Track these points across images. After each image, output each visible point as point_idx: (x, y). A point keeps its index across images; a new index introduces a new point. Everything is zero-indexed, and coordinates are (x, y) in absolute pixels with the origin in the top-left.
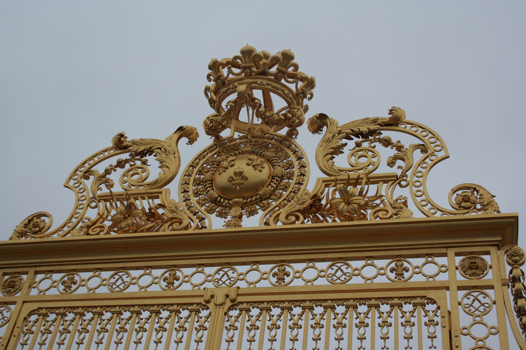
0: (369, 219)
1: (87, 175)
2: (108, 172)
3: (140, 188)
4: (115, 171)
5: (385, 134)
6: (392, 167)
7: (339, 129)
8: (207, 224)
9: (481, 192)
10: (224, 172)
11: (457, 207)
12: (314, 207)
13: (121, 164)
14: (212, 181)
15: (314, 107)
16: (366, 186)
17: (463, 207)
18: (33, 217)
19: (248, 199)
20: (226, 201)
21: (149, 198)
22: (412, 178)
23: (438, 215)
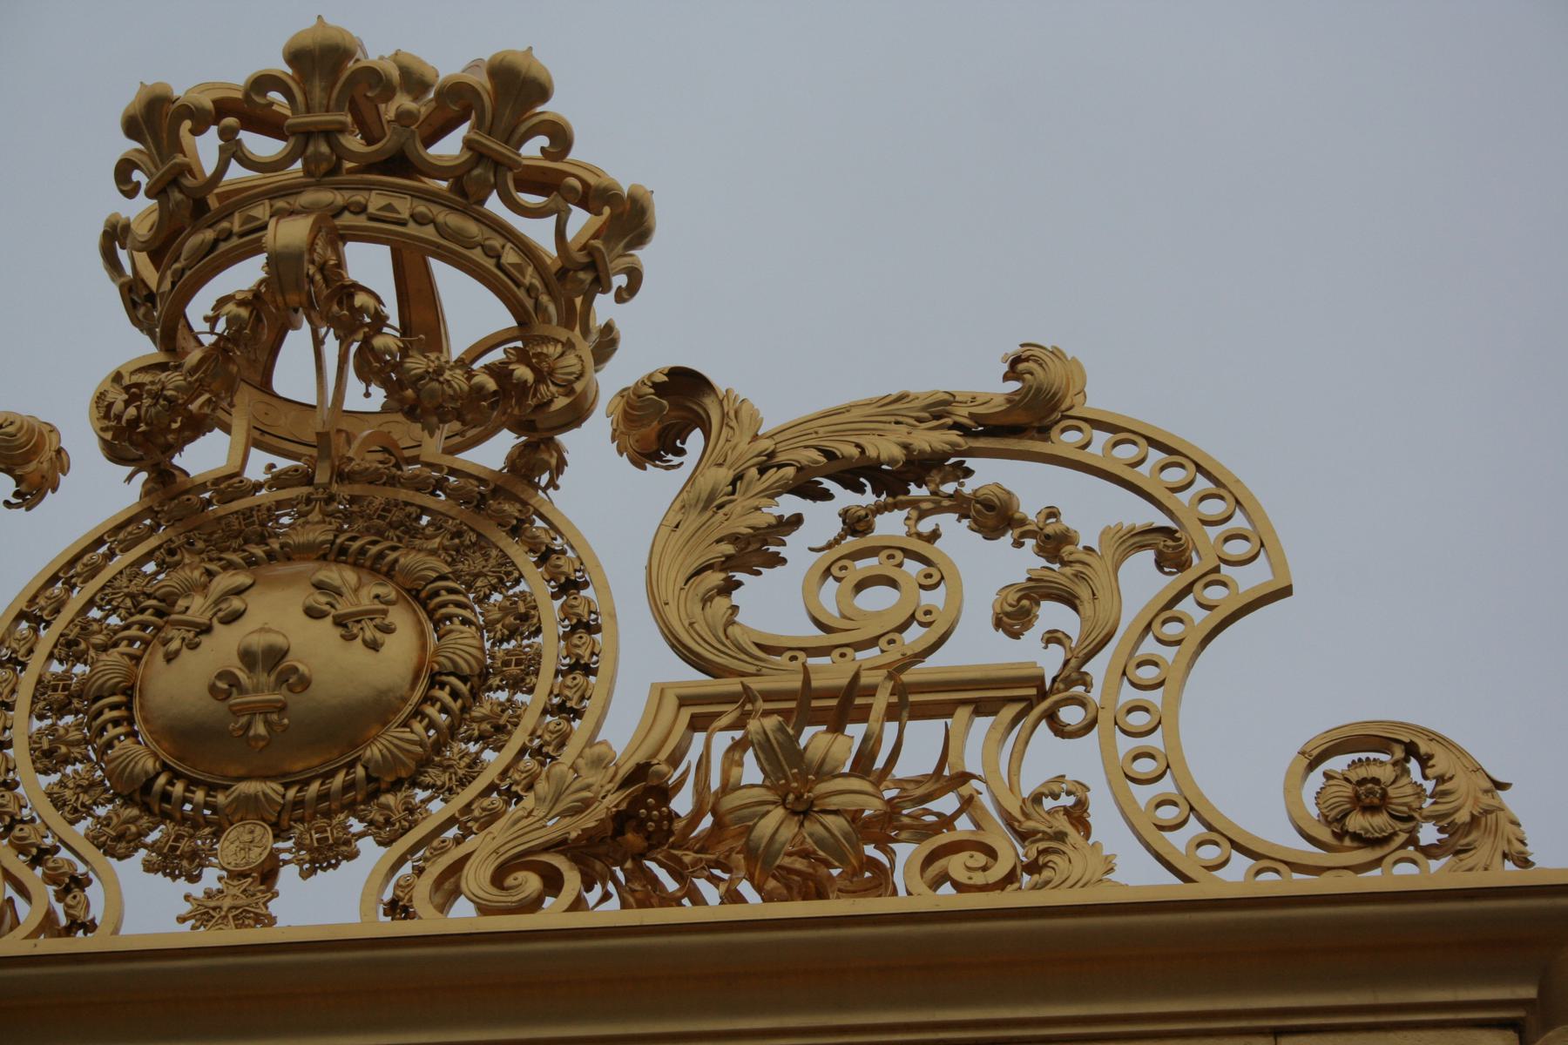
0: (902, 892)
5: (988, 473)
6: (1016, 635)
7: (767, 445)
8: (97, 912)
9: (1441, 764)
10: (194, 646)
11: (1325, 834)
12: (634, 825)
14: (129, 691)
15: (645, 335)
16: (891, 729)
17: (1356, 837)
19: (307, 783)
20: (200, 795)
22: (1111, 691)
23: (1236, 875)
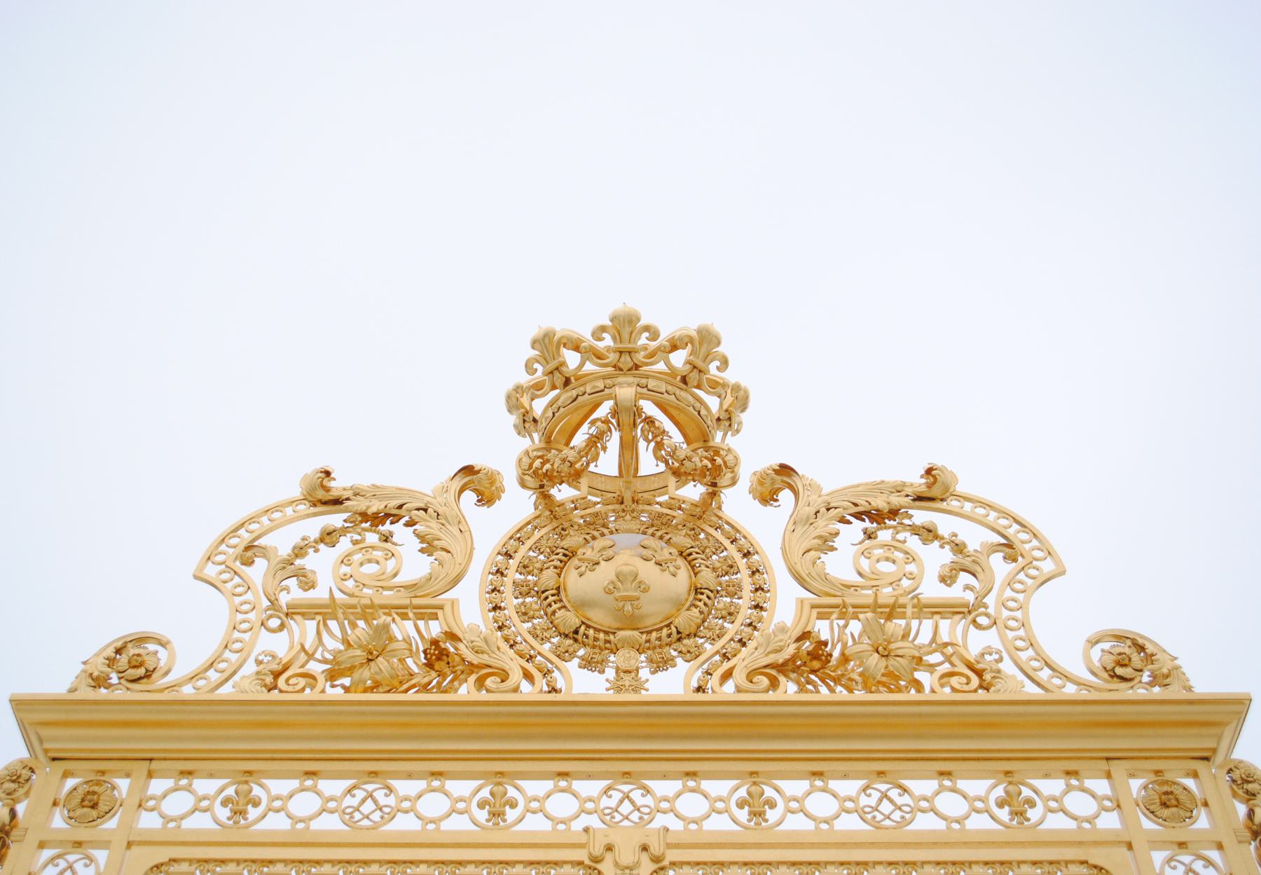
0: (927, 689)
1: (250, 553)
2: (299, 551)
3: (385, 593)
4: (317, 551)
5: (920, 516)
6: (949, 586)
8: (560, 684)
11: (1106, 675)
12: (812, 659)
13: (329, 537)
14: (558, 589)
15: (751, 449)
16: (915, 623)
18: (126, 643)
19: (649, 632)
20: (602, 636)
21: (420, 617)
23: (1070, 690)
